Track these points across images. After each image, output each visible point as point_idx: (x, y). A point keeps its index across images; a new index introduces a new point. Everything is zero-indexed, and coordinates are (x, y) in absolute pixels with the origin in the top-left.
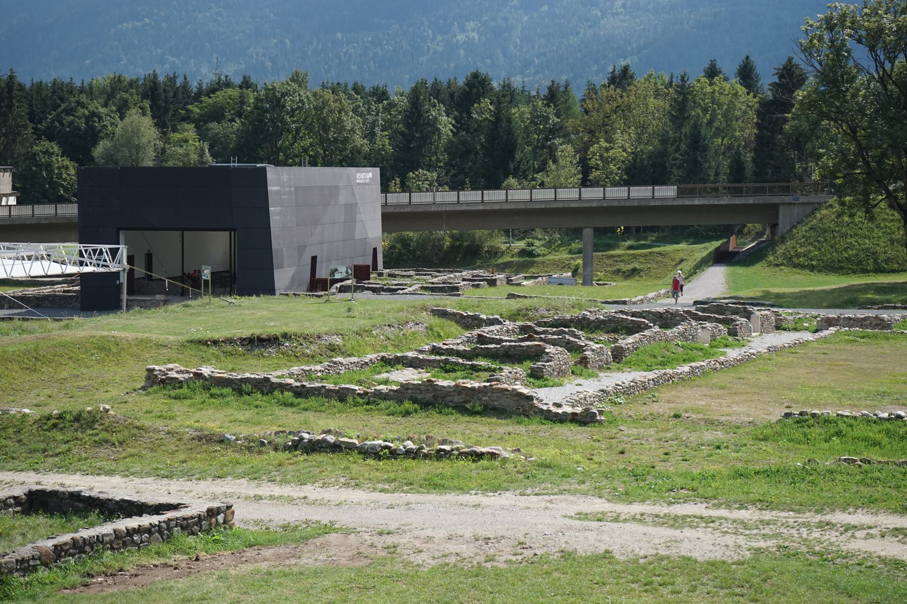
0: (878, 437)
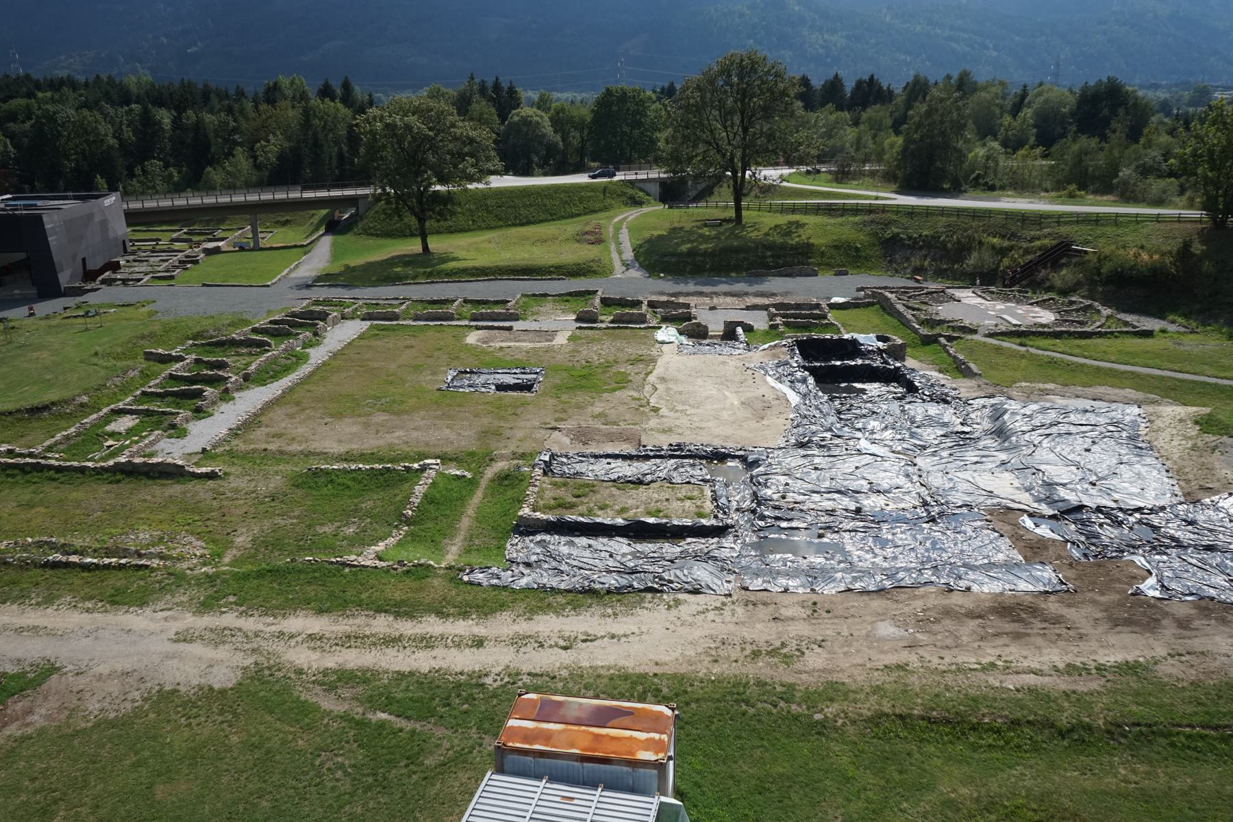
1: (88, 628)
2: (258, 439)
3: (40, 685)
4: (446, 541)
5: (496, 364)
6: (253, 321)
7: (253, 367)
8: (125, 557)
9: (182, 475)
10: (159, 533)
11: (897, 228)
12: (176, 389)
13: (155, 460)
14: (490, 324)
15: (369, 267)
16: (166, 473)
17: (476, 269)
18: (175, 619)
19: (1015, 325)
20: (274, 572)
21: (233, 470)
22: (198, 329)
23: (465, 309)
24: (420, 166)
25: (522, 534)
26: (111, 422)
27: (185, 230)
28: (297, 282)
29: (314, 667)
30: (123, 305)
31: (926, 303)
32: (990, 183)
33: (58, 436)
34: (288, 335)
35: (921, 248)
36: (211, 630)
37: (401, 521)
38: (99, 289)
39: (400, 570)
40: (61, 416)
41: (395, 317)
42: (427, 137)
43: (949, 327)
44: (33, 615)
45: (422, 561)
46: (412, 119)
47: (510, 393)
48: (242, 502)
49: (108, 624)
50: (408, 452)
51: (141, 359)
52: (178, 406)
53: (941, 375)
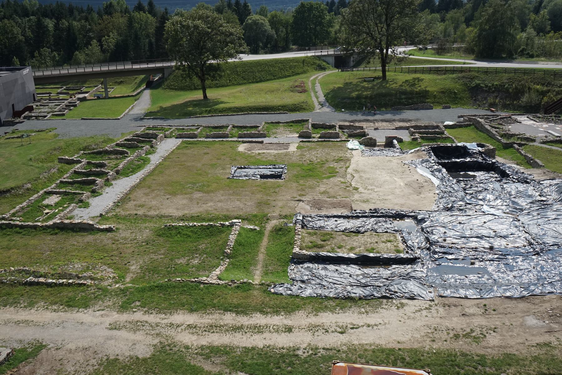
0: (190, 234)
1: (57, 321)
2: (130, 208)
3: (36, 356)
4: (252, 268)
5: (257, 162)
6: (115, 139)
7: (121, 166)
8: (70, 279)
9: (93, 230)
10: (86, 264)
11: (479, 80)
12: (79, 179)
13: (76, 221)
14: (250, 140)
15: (174, 107)
16: (83, 228)
17: (237, 108)
18: (107, 316)
19: (557, 137)
20: (160, 287)
21: (120, 226)
22: (85, 144)
23: (234, 131)
24: (202, 49)
25: (295, 263)
26: (45, 199)
27: (65, 88)
28: (135, 117)
29: (195, 345)
30: (39, 131)
31: (501, 124)
32: (531, 53)
33: (18, 208)
34: (137, 147)
35: (493, 92)
36: (130, 322)
37: (224, 256)
38: (23, 122)
39: (233, 286)
40: (17, 196)
41: (195, 136)
42: (208, 33)
43: (519, 138)
44: (23, 313)
45: (245, 280)
46: (198, 22)
47: (270, 180)
48: (129, 245)
49: (69, 319)
50: (218, 215)
51: (56, 162)
52: (81, 189)
53: (518, 167)
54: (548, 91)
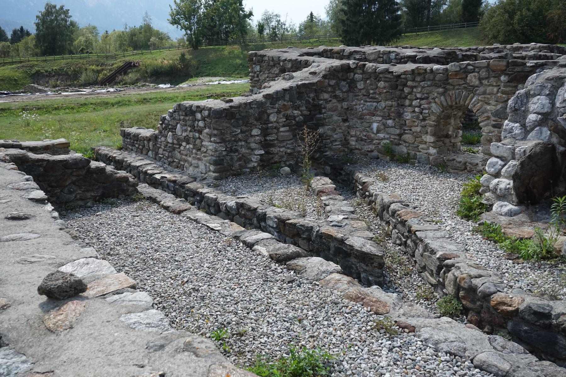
35: (54, 76)
54: (103, 70)
